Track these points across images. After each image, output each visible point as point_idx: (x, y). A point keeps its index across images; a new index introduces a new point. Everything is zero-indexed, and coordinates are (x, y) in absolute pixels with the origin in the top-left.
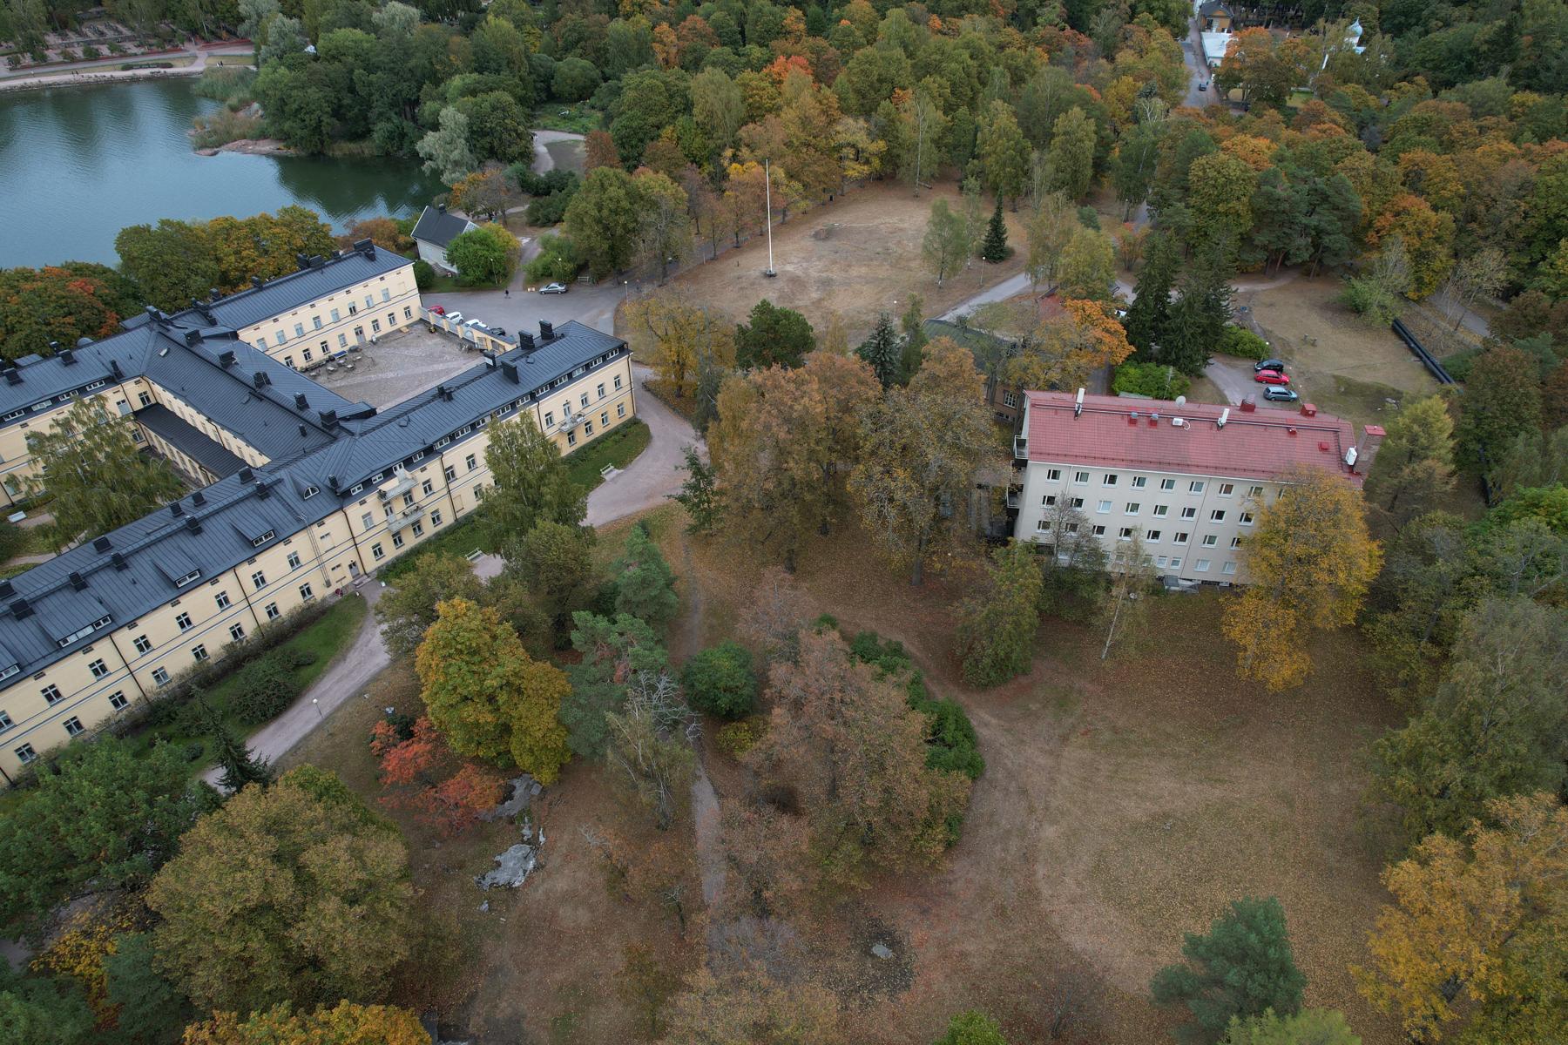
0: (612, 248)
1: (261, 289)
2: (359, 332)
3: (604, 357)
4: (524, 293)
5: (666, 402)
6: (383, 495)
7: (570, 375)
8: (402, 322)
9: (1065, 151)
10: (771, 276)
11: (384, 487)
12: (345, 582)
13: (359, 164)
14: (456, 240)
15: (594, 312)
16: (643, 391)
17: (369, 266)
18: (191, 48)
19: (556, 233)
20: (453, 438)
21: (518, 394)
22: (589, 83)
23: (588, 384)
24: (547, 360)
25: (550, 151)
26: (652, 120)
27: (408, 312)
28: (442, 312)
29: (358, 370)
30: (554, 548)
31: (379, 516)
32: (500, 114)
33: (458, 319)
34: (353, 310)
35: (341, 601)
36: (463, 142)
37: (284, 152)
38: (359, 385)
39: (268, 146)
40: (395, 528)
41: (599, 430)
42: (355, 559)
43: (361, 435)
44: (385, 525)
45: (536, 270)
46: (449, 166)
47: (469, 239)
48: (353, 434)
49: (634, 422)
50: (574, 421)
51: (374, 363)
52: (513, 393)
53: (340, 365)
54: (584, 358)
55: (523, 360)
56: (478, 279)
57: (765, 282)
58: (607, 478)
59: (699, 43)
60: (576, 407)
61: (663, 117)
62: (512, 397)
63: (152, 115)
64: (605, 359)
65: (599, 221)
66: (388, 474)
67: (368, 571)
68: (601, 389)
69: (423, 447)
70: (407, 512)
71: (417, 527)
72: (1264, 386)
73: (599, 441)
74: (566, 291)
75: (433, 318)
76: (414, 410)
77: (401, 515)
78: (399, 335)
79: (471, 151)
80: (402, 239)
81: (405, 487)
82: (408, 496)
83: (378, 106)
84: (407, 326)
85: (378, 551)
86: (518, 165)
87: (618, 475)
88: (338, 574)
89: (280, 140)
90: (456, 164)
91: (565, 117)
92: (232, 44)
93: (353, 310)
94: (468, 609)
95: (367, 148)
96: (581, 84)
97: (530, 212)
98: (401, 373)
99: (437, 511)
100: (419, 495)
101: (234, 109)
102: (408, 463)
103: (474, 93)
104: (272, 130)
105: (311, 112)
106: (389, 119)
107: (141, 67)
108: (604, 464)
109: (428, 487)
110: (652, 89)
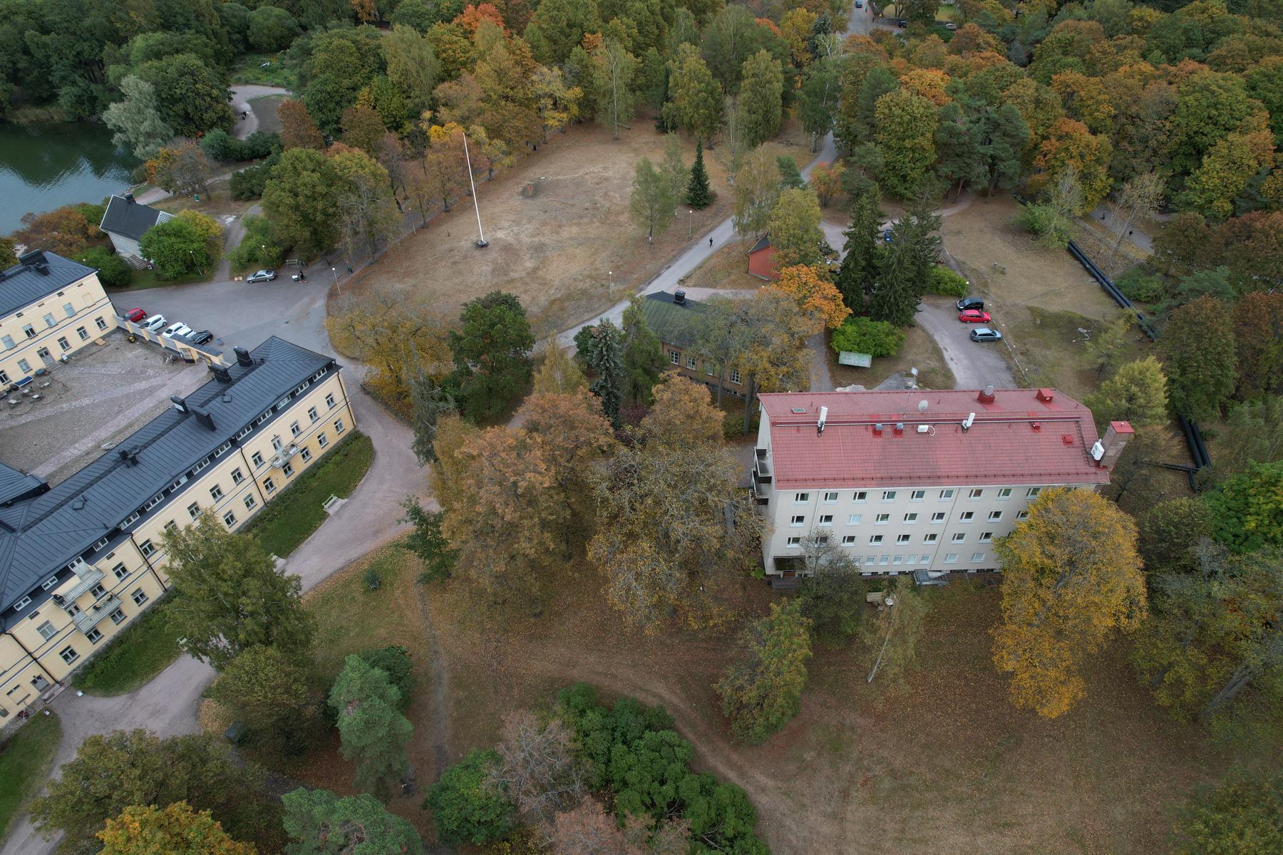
0: (315, 232)
2: (44, 353)
3: (311, 381)
4: (232, 283)
5: (387, 406)
6: (60, 600)
7: (274, 409)
8: (95, 333)
9: (755, 92)
10: (483, 246)
11: (60, 591)
12: (29, 701)
13: (52, 132)
14: (149, 234)
15: (306, 300)
16: (361, 395)
17: (42, 282)
19: (255, 210)
20: (143, 512)
21: (217, 443)
22: (286, 33)
23: (298, 412)
24: (247, 389)
25: (254, 108)
26: (346, 82)
27: (100, 322)
28: (139, 318)
29: (49, 399)
30: (257, 688)
31: (60, 619)
32: (188, 78)
33: (159, 324)
34: (30, 333)
35: (26, 726)
36: (152, 111)
38: (49, 418)
40: (86, 627)
41: (317, 453)
42: (39, 671)
43: (24, 530)
44: (72, 627)
45: (240, 257)
46: (142, 139)
47: (163, 232)
48: (13, 530)
49: (355, 436)
50: (286, 453)
51: (66, 388)
52: (211, 442)
53: (25, 395)
54: (288, 386)
55: (219, 399)
56: (180, 273)
57: (477, 253)
58: (331, 511)
60: (287, 438)
61: (357, 79)
62: (208, 450)
64: (312, 382)
65: (296, 208)
66: (64, 574)
67: (59, 677)
68: (313, 414)
69: (106, 532)
70: (98, 604)
71: (117, 614)
72: (971, 327)
73: (317, 466)
74: (275, 277)
75: (131, 327)
76: (91, 484)
77: (92, 610)
78: (94, 349)
79: (163, 120)
80: (92, 230)
81: (90, 582)
82: (97, 589)
84: (103, 338)
85: (68, 654)
86: (217, 132)
87: (343, 506)
88: (18, 695)
90: (149, 135)
91: (266, 70)
93: (30, 333)
94: (144, 824)
96: (278, 33)
97: (235, 184)
98: (98, 398)
99: (139, 590)
100: (111, 583)
102: (89, 555)
103: (158, 55)
106: (74, 83)
108: (325, 497)
109: (121, 571)
110: (342, 49)
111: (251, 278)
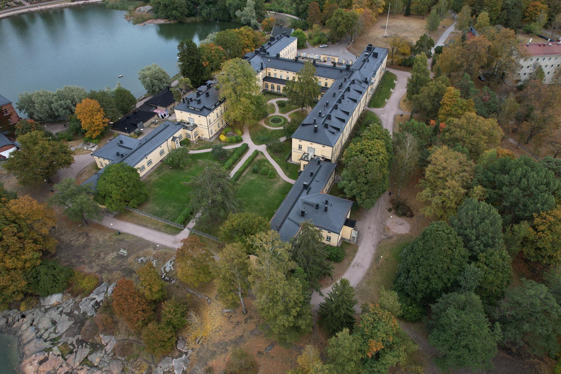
1: (271, 45)
37: (168, 22)
39: (162, 21)
89: (165, 19)
90: (253, 17)
95: (198, 19)
104: (162, 15)
105: (181, 8)
111: (321, 46)
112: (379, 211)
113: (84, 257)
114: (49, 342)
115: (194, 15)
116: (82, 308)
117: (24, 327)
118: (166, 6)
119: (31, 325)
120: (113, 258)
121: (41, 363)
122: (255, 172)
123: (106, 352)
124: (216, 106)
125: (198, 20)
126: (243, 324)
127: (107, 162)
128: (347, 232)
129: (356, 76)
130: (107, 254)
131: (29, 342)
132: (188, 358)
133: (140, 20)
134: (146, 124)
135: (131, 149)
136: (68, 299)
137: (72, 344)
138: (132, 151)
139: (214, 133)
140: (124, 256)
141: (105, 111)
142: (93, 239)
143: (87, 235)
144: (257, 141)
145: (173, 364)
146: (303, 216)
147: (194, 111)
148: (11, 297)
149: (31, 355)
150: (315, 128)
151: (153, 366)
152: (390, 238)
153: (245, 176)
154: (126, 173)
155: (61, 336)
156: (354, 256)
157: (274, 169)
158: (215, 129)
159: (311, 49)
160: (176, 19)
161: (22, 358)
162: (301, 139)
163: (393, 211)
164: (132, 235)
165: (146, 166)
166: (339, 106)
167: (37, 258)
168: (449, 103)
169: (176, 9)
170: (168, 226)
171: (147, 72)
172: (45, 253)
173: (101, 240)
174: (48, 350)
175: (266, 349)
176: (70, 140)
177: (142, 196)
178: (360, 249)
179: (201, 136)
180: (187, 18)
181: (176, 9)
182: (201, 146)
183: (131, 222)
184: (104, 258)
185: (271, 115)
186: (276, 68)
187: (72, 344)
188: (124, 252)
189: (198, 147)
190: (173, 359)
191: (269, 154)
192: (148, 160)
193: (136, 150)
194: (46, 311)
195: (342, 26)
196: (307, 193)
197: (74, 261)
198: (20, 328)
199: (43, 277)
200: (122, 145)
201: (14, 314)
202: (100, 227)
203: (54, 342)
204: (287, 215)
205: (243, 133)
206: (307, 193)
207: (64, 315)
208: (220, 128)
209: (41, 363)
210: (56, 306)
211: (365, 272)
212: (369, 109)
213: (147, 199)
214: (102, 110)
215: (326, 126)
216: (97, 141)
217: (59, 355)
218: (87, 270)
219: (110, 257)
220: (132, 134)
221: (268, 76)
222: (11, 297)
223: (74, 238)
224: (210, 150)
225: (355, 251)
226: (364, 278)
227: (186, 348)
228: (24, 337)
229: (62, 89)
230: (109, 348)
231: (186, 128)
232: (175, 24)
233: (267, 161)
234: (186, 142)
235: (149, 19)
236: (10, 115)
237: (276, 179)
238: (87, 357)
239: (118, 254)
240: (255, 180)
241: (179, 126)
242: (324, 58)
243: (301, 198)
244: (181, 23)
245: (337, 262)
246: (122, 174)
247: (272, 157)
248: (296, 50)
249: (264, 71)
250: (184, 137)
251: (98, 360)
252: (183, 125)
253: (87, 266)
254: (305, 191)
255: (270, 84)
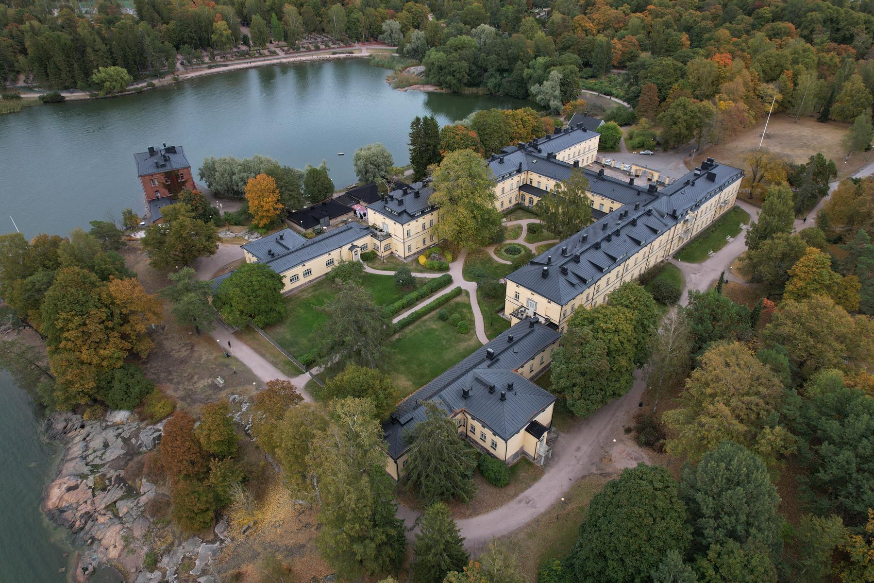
1: (550, 140)
8: (590, 162)
18: (357, 46)
26: (668, 81)
37: (439, 91)
39: (430, 89)
59: (633, 49)
61: (672, 79)
63: (328, 75)
83: (491, 70)
84: (592, 164)
89: (436, 85)
90: (555, 97)
92: (374, 44)
95: (481, 91)
101: (401, 72)
106: (496, 78)
107: (340, 53)
110: (668, 66)
111: (642, 152)
112: (609, 427)
113: (175, 374)
114: (89, 468)
115: (477, 85)
116: (142, 436)
117: (78, 439)
118: (441, 68)
119: (84, 439)
120: (205, 386)
121: (69, 489)
122: (443, 318)
123: (138, 503)
124: (423, 213)
125: (480, 93)
126: (313, 529)
127: (255, 259)
128: (534, 446)
129: (662, 205)
130: (201, 378)
131: (72, 459)
132: (222, 548)
133: (402, 85)
134: (332, 222)
135: (288, 249)
136: (133, 421)
137: (110, 479)
138: (288, 252)
139: (414, 250)
140: (218, 387)
141: (281, 193)
142: (196, 355)
143: (192, 349)
144: (468, 274)
145: (200, 550)
146: (465, 398)
147: (390, 215)
148: (75, 397)
149: (65, 476)
150: (544, 270)
151: (177, 542)
152: (604, 475)
153: (426, 321)
154: (259, 279)
155: (104, 465)
156: (530, 486)
157: (472, 322)
158: (416, 245)
159: (626, 155)
160: (449, 87)
161: (57, 475)
162: (519, 283)
163: (633, 433)
164: (241, 362)
165: (301, 276)
166: (604, 245)
167: (119, 358)
168: (803, 275)
169: (452, 73)
170: (289, 363)
171: (363, 153)
172: (133, 356)
173: (204, 358)
174: (83, 477)
175: (326, 577)
176: (236, 225)
177: (273, 314)
178: (546, 477)
179: (394, 252)
180: (466, 88)
181: (452, 73)
182: (390, 265)
183: (250, 346)
184: (195, 383)
185: (508, 242)
186: (541, 173)
187: (110, 479)
188: (220, 381)
189: (384, 266)
190: (202, 542)
191: (477, 298)
192: (306, 268)
193: (293, 252)
194: (107, 427)
195: (680, 126)
196: (489, 366)
197: (162, 375)
198: (73, 439)
199: (116, 384)
200: (282, 242)
201: (76, 419)
202: (211, 341)
203: (95, 468)
204: (441, 390)
205: (454, 259)
206: (489, 366)
207: (119, 439)
208: (425, 246)
209: (69, 489)
210: (117, 426)
211: (535, 516)
212: (674, 262)
213: (280, 320)
214: (277, 191)
215: (564, 272)
216: (264, 231)
217: (90, 488)
218: (170, 392)
219: (202, 383)
220: (310, 231)
221: (528, 183)
222: (75, 397)
223: (177, 348)
224: (392, 273)
225: (535, 478)
226: (528, 525)
227: (226, 533)
228: (71, 451)
229: (250, 158)
230: (143, 499)
231: (374, 236)
232: (447, 94)
233: (469, 307)
234: (369, 257)
235: (416, 84)
236: (185, 182)
237: (466, 336)
238: (115, 502)
239: (213, 382)
240: (436, 330)
241: (366, 232)
242: (636, 171)
243: (475, 370)
244: (456, 93)
245: (496, 485)
246: (254, 278)
247: (479, 303)
248: (595, 153)
249: (523, 176)
250: (370, 248)
251: (125, 510)
252: (373, 231)
253: (172, 387)
254: (488, 362)
255: (528, 196)
